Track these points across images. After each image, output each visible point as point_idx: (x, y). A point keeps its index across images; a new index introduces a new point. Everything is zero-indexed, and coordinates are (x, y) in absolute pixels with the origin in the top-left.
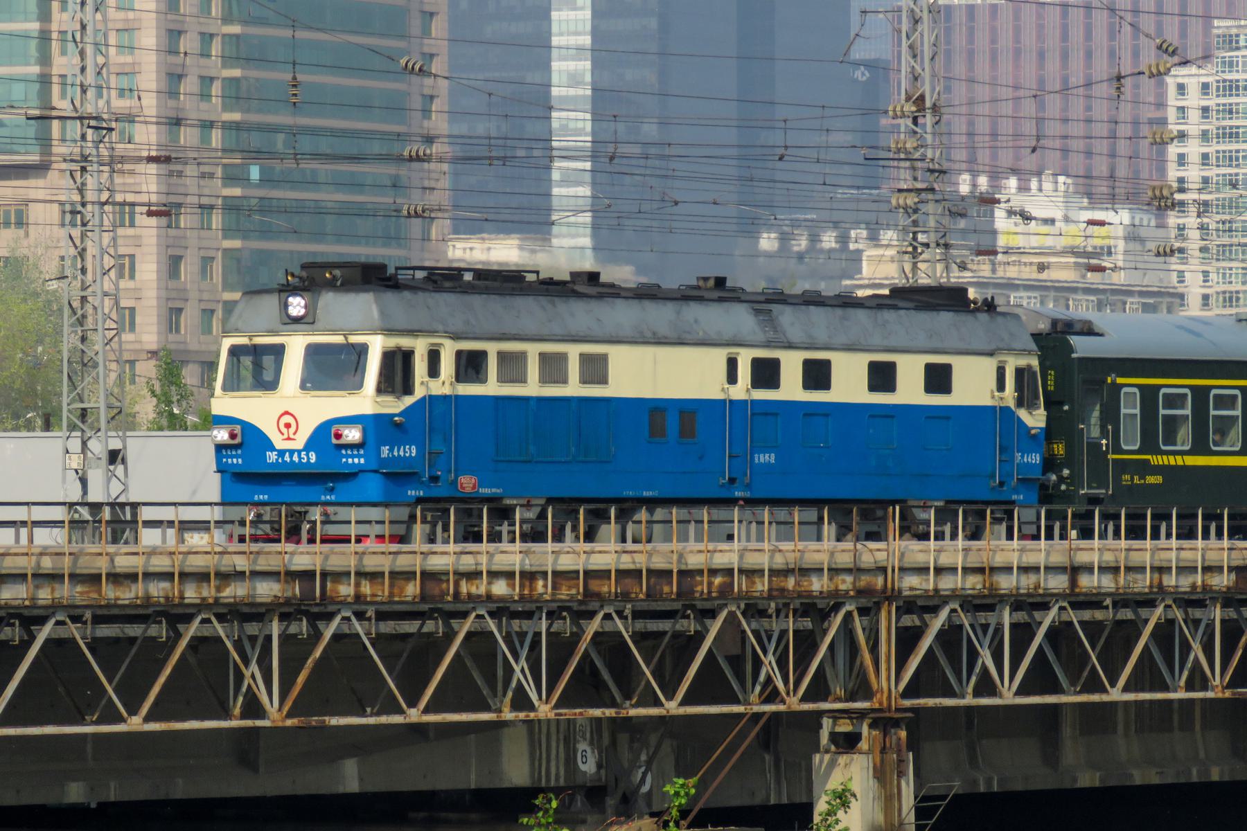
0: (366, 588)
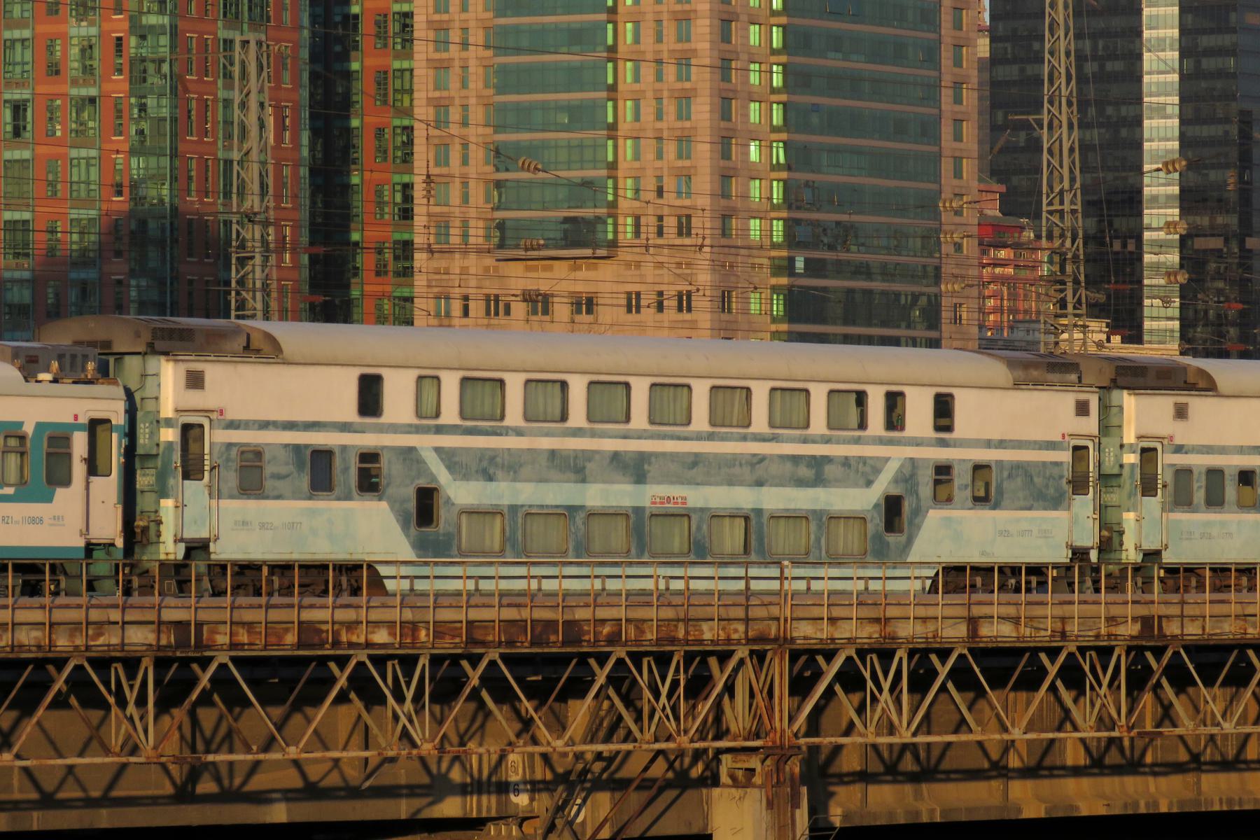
0: (243, 637)
